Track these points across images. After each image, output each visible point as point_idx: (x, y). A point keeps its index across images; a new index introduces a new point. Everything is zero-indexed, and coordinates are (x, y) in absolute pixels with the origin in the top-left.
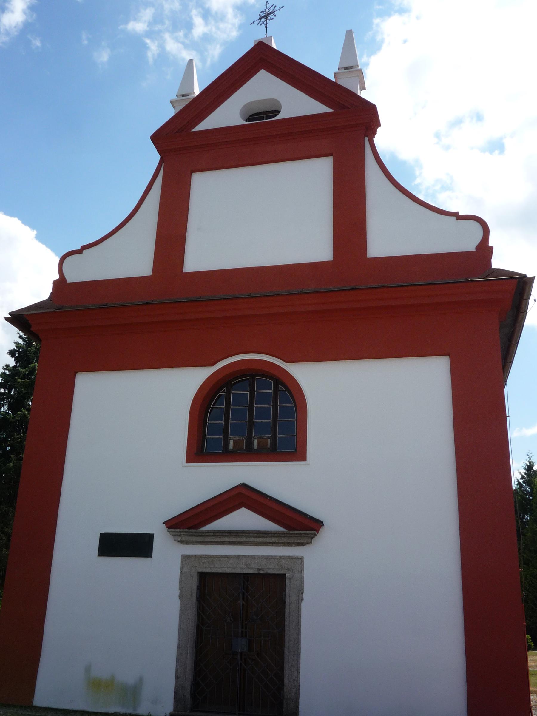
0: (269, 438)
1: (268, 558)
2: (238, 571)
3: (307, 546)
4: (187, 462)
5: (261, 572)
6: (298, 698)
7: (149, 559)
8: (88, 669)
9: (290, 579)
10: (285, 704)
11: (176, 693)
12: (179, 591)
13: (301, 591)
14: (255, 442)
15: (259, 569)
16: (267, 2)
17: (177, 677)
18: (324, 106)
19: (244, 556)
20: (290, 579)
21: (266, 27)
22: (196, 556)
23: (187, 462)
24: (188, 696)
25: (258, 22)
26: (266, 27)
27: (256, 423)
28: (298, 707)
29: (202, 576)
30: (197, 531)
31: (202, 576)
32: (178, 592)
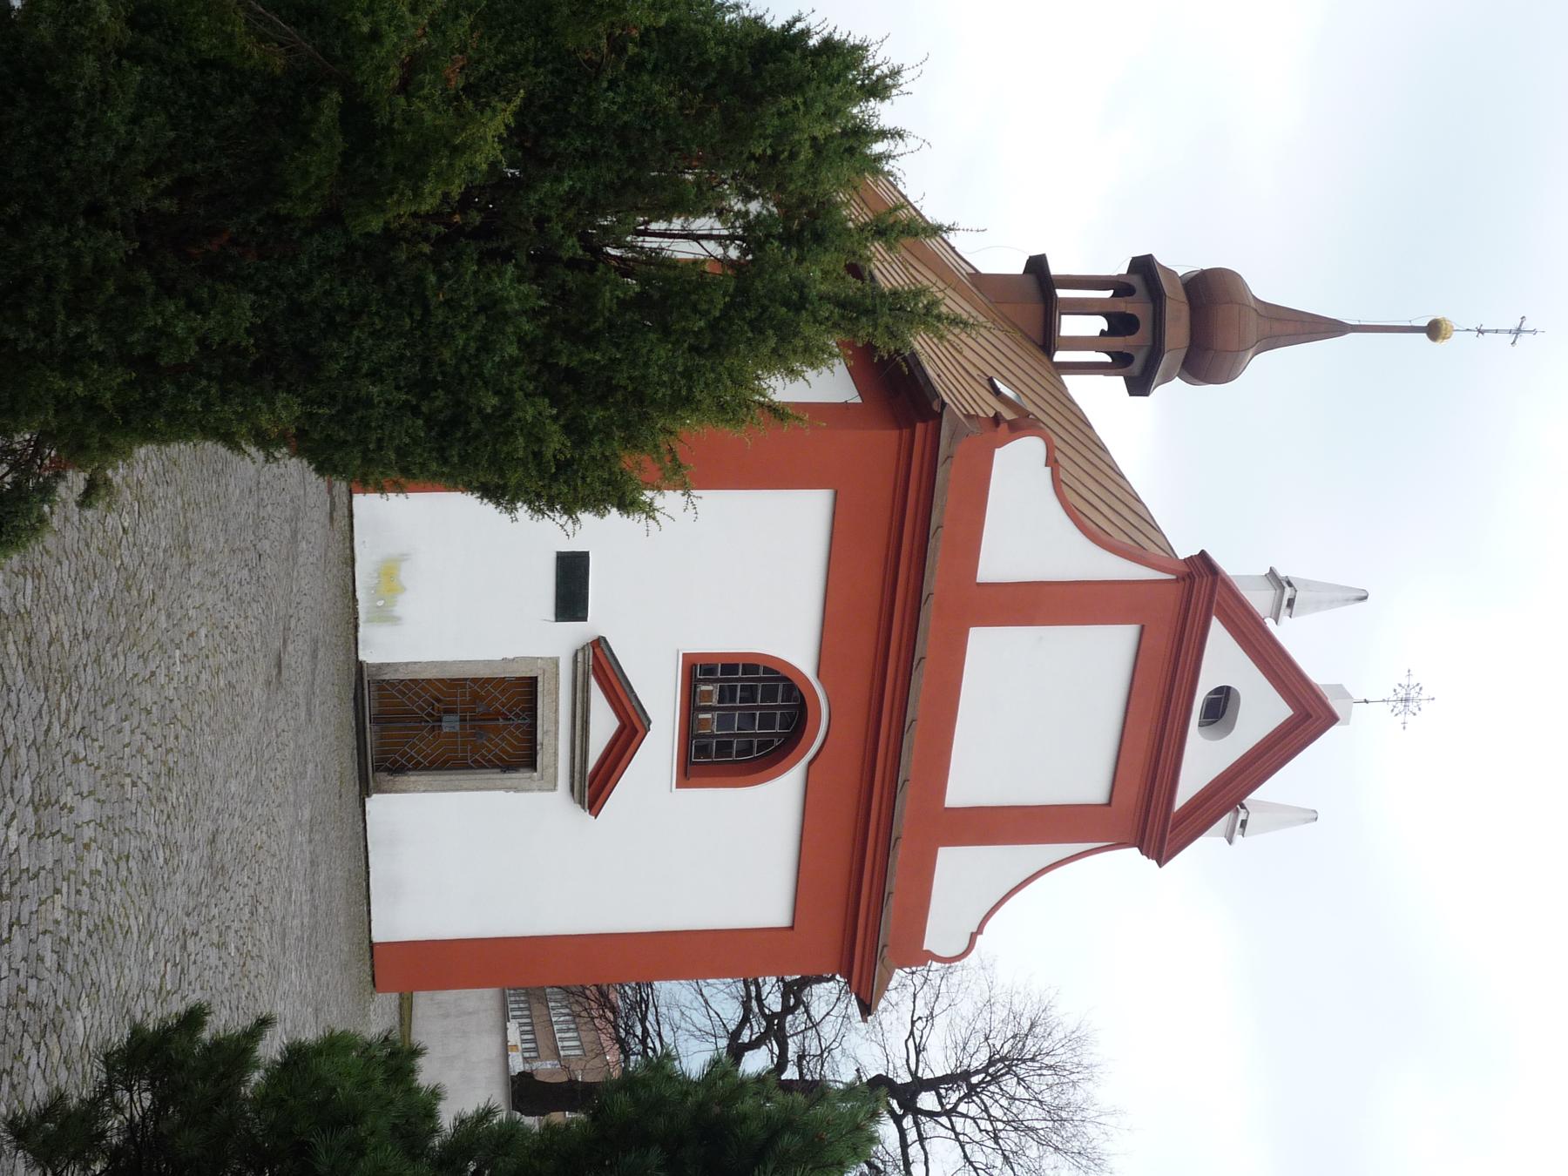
0: (713, 731)
1: (556, 754)
2: (539, 722)
3: (569, 794)
4: (684, 654)
5: (538, 747)
6: (396, 792)
7: (553, 618)
8: (404, 557)
9: (530, 778)
10: (389, 778)
11: (388, 664)
12: (512, 657)
13: (517, 790)
14: (708, 716)
15: (542, 744)
16: (1433, 699)
17: (407, 664)
18: (1183, 804)
19: (557, 729)
20: (530, 778)
21: (1384, 701)
22: (557, 674)
23: (684, 654)
24: (386, 677)
25: (1404, 683)
26: (1384, 701)
27: (734, 715)
28: (386, 792)
29: (532, 682)
30: (591, 672)
31: (532, 682)
32: (511, 656)
